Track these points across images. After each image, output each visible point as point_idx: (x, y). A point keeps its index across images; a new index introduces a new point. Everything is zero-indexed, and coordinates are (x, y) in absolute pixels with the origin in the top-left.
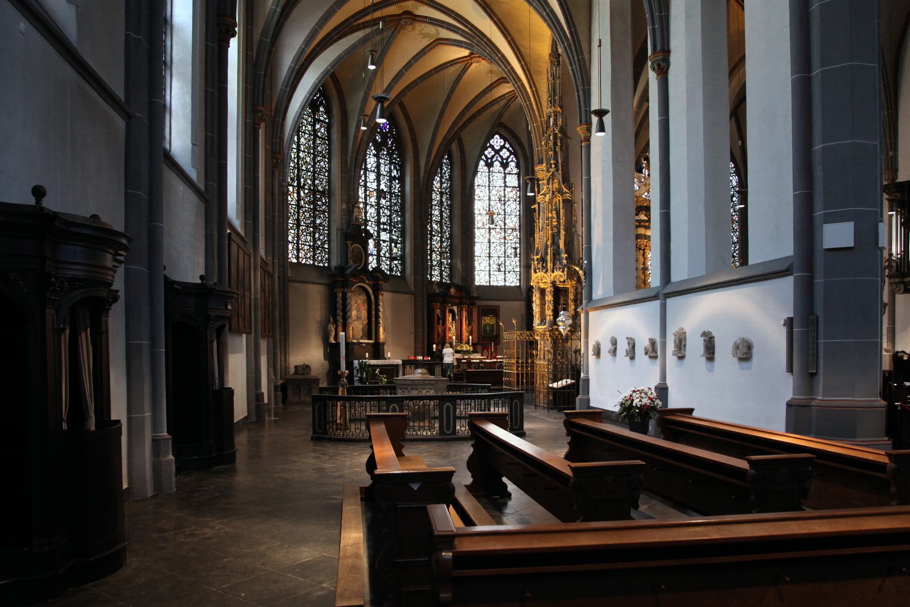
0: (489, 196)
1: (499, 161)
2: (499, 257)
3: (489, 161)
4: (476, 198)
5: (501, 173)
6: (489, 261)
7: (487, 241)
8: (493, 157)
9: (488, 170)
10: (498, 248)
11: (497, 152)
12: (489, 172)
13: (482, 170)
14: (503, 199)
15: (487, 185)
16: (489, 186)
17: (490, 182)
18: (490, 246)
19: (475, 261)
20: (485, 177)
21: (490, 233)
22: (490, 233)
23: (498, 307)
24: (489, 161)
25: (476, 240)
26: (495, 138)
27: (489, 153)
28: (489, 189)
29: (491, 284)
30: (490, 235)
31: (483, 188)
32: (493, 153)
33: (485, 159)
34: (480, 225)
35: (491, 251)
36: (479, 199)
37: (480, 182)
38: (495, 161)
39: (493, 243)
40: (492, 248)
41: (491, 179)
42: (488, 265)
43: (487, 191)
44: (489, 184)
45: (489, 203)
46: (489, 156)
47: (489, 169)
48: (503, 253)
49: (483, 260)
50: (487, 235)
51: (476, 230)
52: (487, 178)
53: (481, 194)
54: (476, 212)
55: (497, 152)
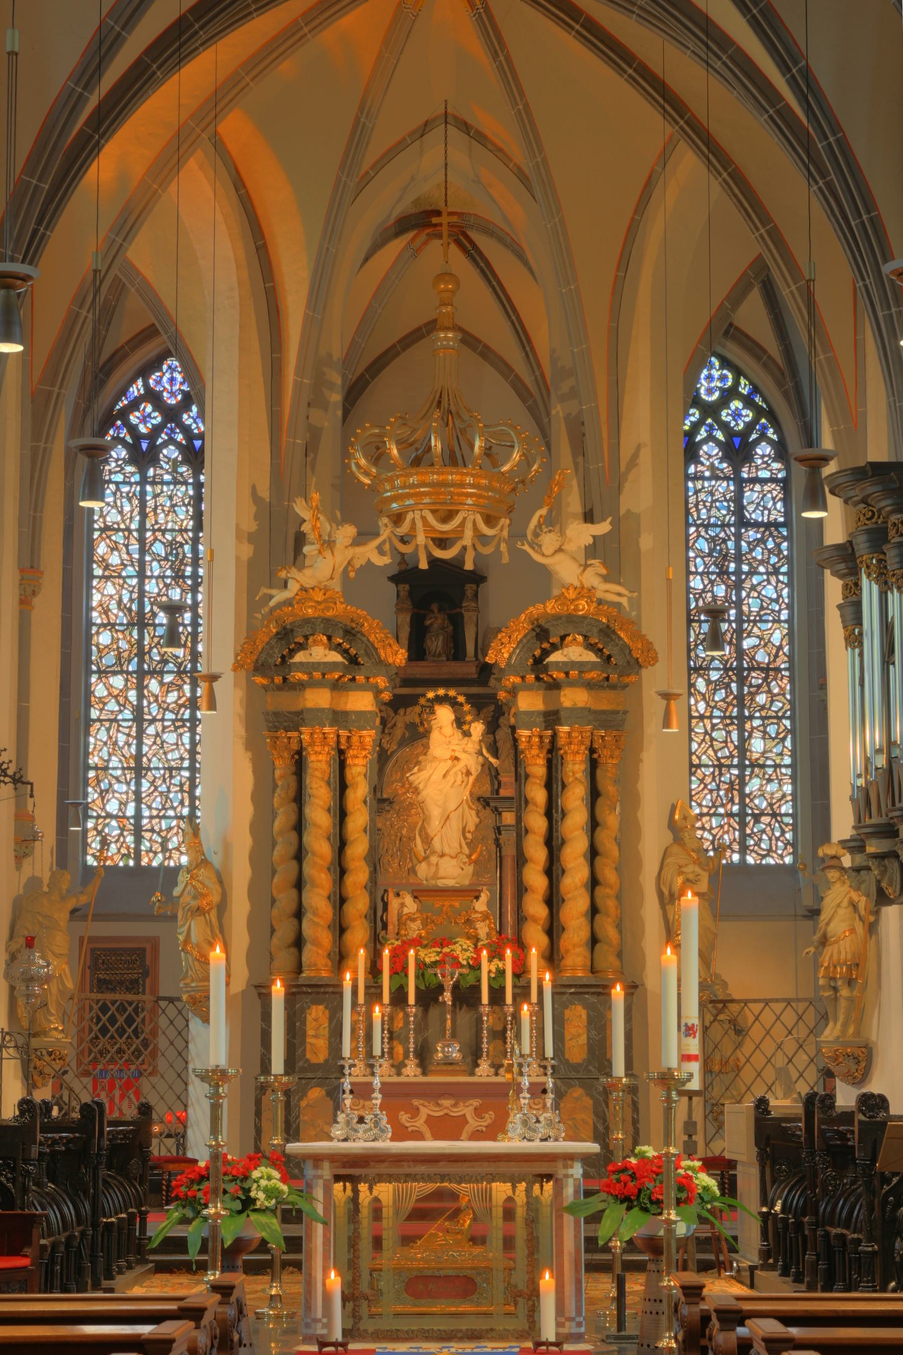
0: (142, 563)
1: (178, 445)
2: (170, 769)
3: (144, 445)
4: (98, 572)
5: (185, 483)
6: (138, 784)
7: (128, 714)
8: (156, 430)
9: (136, 478)
10: (170, 738)
11: (172, 415)
12: (143, 482)
13: (119, 478)
14: (189, 570)
15: (134, 526)
16: (142, 529)
17: (143, 515)
18: (141, 733)
19: (86, 783)
20: (130, 500)
21: (141, 688)
22: (141, 688)
23: (155, 943)
24: (144, 445)
25: (94, 714)
26: (165, 367)
27: (144, 419)
28: (142, 541)
29: (144, 862)
30: (140, 697)
31: (119, 537)
32: (157, 419)
33: (129, 439)
34: (109, 660)
35: (145, 749)
36: (106, 573)
37: (113, 517)
38: (165, 444)
39: (153, 721)
40: (148, 741)
41: (151, 504)
42: (132, 796)
43: (135, 547)
44: (142, 523)
45: (141, 584)
46: (143, 429)
47: (143, 472)
48: (186, 755)
49: (114, 781)
50: (132, 695)
51: (94, 679)
52: (136, 502)
53: (114, 559)
54: (96, 617)
55: (172, 415)
